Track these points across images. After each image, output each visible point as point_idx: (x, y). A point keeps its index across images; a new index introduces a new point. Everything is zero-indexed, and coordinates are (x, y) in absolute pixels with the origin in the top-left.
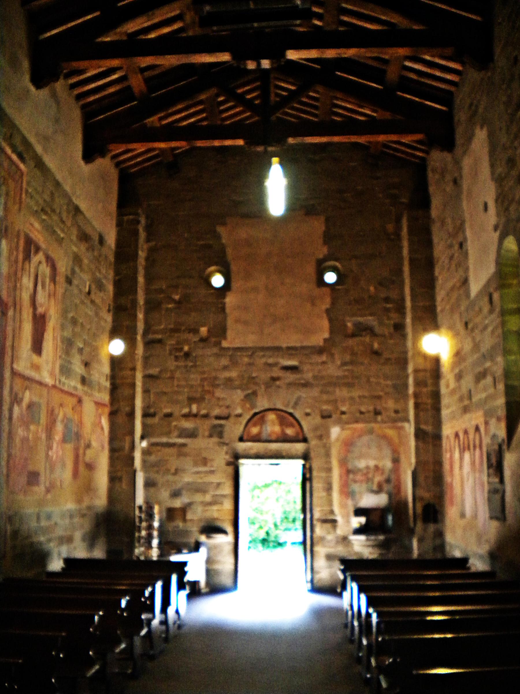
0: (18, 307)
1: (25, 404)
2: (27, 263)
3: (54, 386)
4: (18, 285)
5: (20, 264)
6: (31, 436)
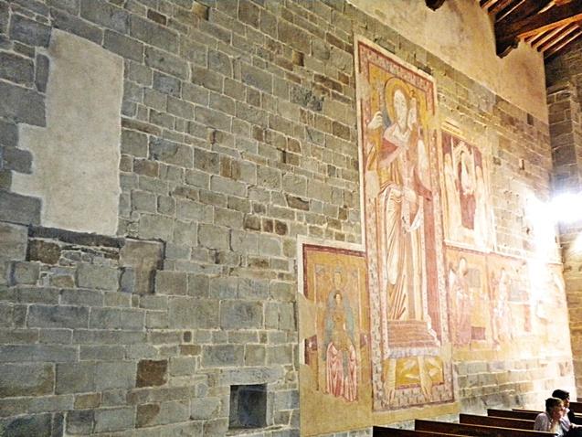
0: (443, 192)
1: (460, 271)
2: (448, 155)
3: (491, 253)
4: (441, 175)
5: (441, 158)
6: (471, 298)
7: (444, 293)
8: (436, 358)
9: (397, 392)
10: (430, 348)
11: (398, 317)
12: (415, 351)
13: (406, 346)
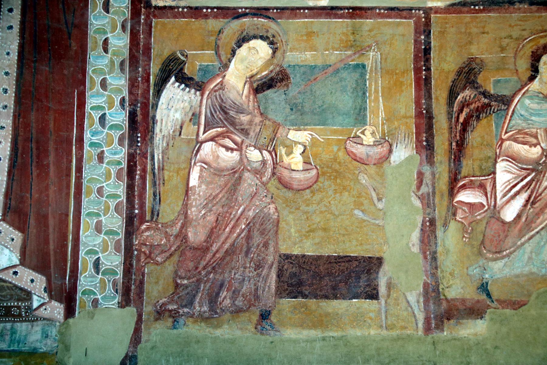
7: (119, 154)
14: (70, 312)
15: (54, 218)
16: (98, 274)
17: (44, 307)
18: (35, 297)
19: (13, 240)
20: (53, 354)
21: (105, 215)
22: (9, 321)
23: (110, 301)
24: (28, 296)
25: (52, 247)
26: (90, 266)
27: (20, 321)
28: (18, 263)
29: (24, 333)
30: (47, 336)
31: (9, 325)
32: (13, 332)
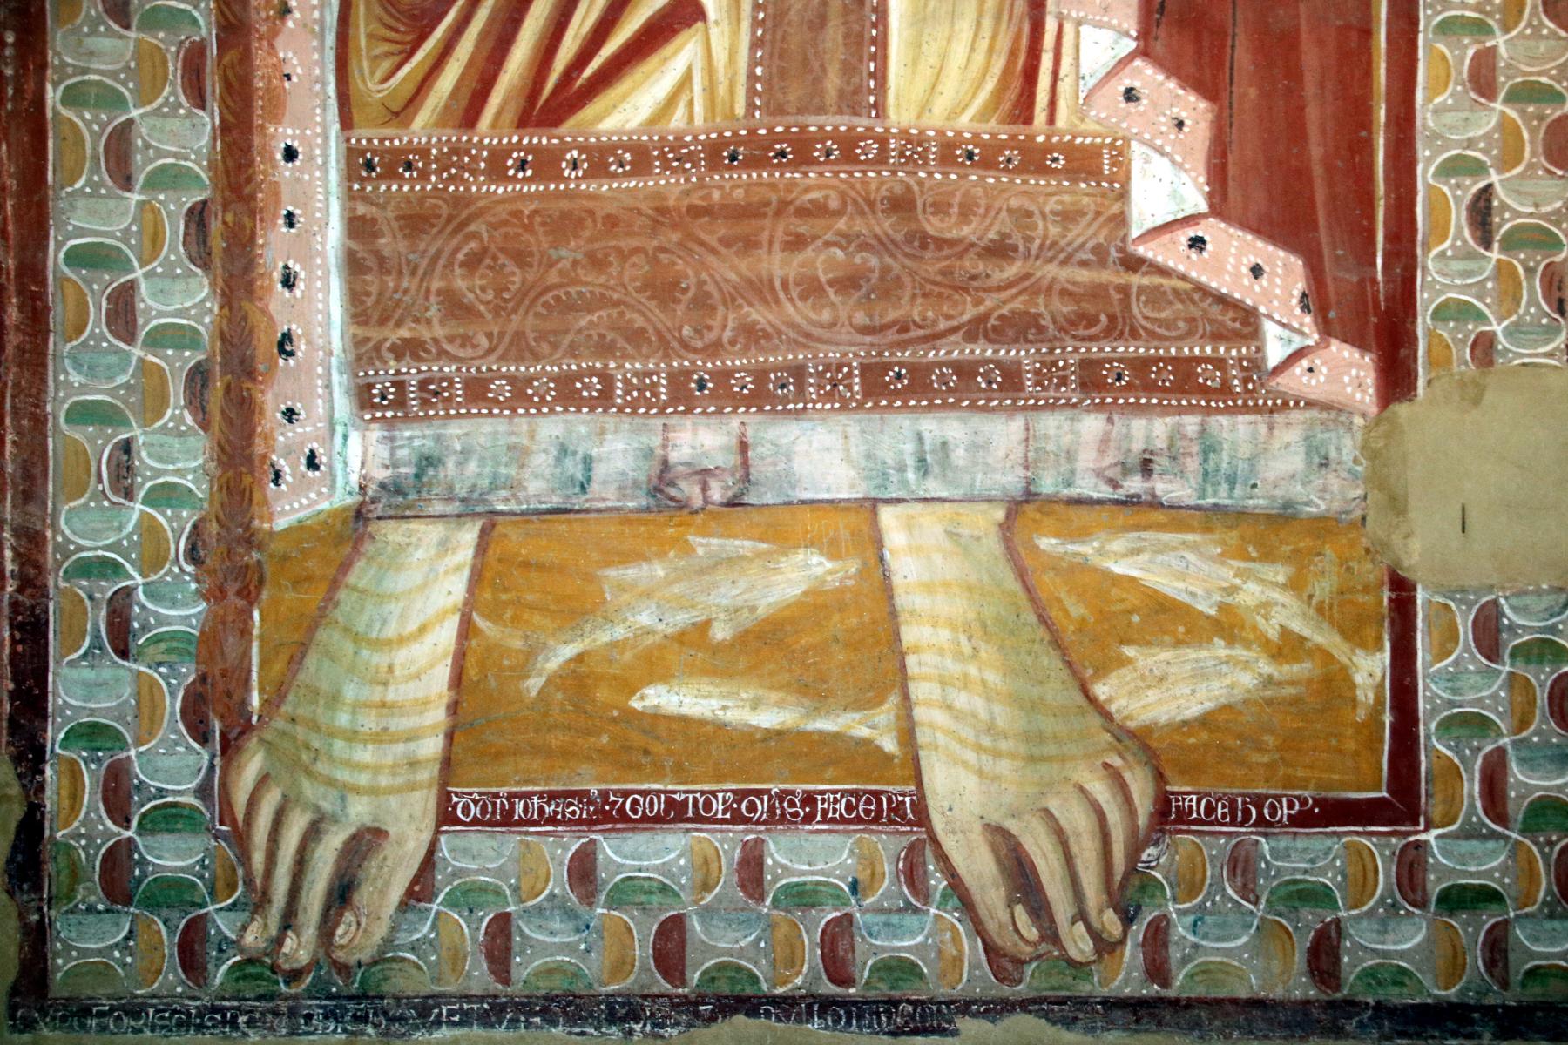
8: (1269, 530)
9: (479, 856)
10: (1149, 430)
11: (551, 104)
12: (821, 454)
13: (685, 396)
14: (1396, 379)
15: (1321, 43)
16: (1488, 247)
17: (1305, 363)
18: (1271, 330)
19: (1180, 124)
20: (1352, 524)
21: (1506, 29)
22: (1191, 409)
23: (1536, 344)
24: (1247, 322)
25: (1316, 151)
26: (1458, 217)
27: (1227, 411)
28: (1203, 207)
29: (1245, 451)
30: (1325, 464)
31: (1191, 423)
32: (1209, 448)
